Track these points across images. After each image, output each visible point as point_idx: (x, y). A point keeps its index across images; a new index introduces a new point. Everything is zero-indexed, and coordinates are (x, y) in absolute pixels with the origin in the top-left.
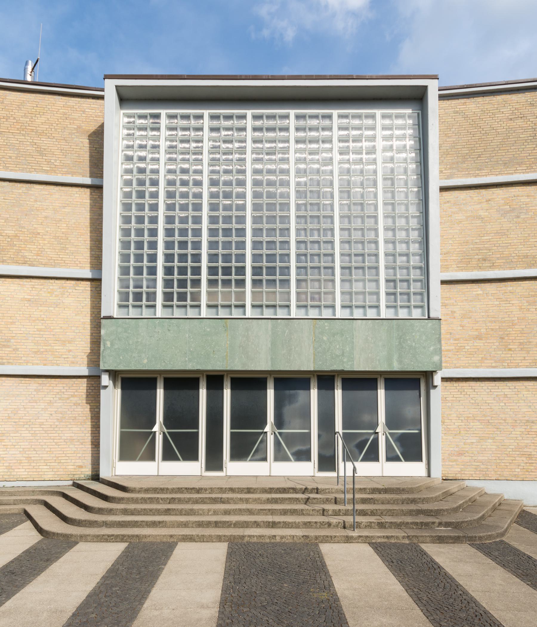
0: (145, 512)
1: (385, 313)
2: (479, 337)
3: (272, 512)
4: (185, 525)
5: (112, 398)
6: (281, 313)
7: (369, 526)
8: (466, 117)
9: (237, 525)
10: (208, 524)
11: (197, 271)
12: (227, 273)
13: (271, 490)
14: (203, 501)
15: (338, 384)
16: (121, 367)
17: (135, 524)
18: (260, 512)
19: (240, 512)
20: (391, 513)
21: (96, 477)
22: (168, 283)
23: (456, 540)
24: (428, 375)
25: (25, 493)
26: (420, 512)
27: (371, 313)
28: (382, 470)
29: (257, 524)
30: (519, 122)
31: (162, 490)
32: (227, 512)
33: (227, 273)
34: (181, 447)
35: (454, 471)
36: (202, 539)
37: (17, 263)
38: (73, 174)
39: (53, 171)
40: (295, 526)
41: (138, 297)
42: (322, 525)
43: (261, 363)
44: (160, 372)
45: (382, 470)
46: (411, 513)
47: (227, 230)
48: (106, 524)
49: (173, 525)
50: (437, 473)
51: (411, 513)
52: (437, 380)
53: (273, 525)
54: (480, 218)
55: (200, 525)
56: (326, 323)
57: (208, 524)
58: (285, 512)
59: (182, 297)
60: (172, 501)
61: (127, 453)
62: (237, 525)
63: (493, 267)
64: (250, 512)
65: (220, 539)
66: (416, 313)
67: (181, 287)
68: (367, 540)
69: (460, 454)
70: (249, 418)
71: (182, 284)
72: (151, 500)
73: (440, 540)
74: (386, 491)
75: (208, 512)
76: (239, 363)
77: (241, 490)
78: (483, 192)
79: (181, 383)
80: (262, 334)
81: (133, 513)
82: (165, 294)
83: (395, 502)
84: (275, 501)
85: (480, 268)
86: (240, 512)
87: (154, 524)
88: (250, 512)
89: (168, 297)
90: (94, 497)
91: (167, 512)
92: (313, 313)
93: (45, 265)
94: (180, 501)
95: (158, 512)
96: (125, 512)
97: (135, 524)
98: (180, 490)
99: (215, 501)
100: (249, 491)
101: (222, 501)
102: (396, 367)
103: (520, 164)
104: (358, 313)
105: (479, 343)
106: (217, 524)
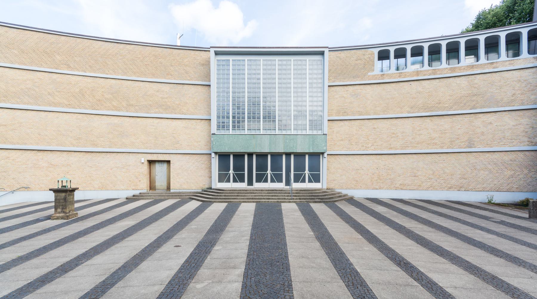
0: (231, 196)
1: (309, 132)
2: (342, 140)
3: (269, 196)
4: (243, 199)
5: (215, 161)
6: (273, 132)
7: (297, 199)
8: (340, 59)
9: (258, 199)
10: (250, 199)
11: (244, 118)
12: (254, 117)
13: (269, 190)
14: (248, 193)
15: (292, 157)
16: (219, 151)
17: (229, 199)
18: (265, 196)
19: (259, 196)
20: (303, 196)
21: (211, 188)
22: (234, 122)
23: (320, 202)
24: (323, 153)
25: (188, 193)
26: (312, 196)
27: (304, 132)
28: (307, 185)
29: (264, 199)
30: (359, 61)
31: (235, 190)
32: (255, 196)
33: (254, 117)
34: (239, 178)
35: (332, 186)
36: (248, 202)
37: (180, 114)
38: (198, 80)
39: (191, 80)
40: (275, 199)
41: (223, 127)
42: (283, 199)
43: (266, 150)
44: (232, 153)
45: (307, 185)
46: (309, 196)
47: (255, 104)
48: (220, 199)
49: (240, 199)
50: (325, 187)
51: (309, 196)
52: (325, 155)
53: (269, 199)
54: (343, 97)
55: (248, 199)
56: (288, 136)
57: (250, 199)
58: (272, 196)
59: (239, 127)
60: (238, 193)
61: (220, 180)
62: (258, 199)
63: (347, 115)
64: (262, 196)
65: (253, 202)
66: (320, 132)
67: (238, 123)
68: (295, 202)
69: (334, 180)
70: (262, 167)
71: (239, 122)
72: (232, 193)
73: (316, 202)
74: (304, 190)
75: (250, 196)
76: (258, 150)
77: (259, 190)
78: (345, 87)
79: (239, 156)
80: (266, 139)
81: (227, 196)
82: (233, 125)
83: (306, 193)
84: (270, 193)
85: (343, 115)
86: (259, 196)
87: (234, 199)
88: (262, 196)
89: (234, 127)
90: (207, 196)
91: (238, 196)
92: (284, 132)
93: (190, 114)
94: (241, 193)
95: (235, 196)
96: (225, 196)
97: (229, 199)
98: (240, 190)
99: (251, 193)
100: (262, 190)
101: (254, 193)
102: (311, 151)
103: (358, 77)
104: (299, 132)
105: (342, 142)
106: (252, 199)
